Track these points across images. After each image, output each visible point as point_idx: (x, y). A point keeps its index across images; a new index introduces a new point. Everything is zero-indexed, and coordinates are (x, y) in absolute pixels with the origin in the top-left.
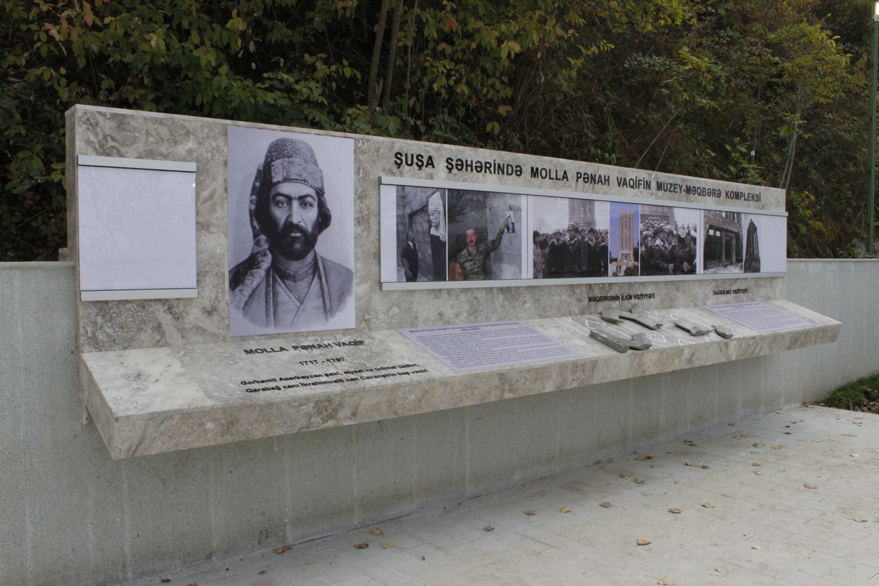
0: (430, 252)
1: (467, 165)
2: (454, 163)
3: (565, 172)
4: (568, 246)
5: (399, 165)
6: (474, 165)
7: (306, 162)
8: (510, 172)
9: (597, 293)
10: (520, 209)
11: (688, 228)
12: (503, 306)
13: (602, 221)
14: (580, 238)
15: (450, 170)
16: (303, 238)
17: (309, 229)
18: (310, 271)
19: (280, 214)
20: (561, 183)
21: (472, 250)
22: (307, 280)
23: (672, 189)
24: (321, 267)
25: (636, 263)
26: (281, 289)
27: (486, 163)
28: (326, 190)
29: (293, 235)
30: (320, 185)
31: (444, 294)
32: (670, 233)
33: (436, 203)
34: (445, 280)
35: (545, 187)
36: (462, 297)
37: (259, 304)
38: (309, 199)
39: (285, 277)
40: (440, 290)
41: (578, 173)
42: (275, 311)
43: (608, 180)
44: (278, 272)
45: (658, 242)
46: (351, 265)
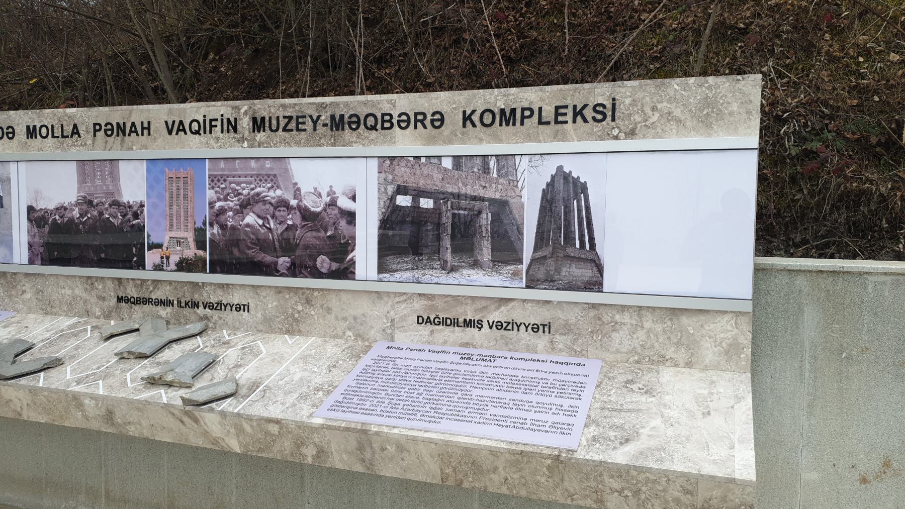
3: (75, 126)
4: (77, 225)
9: (132, 292)
10: (9, 180)
11: (331, 193)
13: (133, 186)
14: (95, 213)
20: (69, 141)
23: (292, 125)
25: (200, 253)
32: (283, 204)
41: (95, 125)
43: (149, 128)
45: (250, 219)
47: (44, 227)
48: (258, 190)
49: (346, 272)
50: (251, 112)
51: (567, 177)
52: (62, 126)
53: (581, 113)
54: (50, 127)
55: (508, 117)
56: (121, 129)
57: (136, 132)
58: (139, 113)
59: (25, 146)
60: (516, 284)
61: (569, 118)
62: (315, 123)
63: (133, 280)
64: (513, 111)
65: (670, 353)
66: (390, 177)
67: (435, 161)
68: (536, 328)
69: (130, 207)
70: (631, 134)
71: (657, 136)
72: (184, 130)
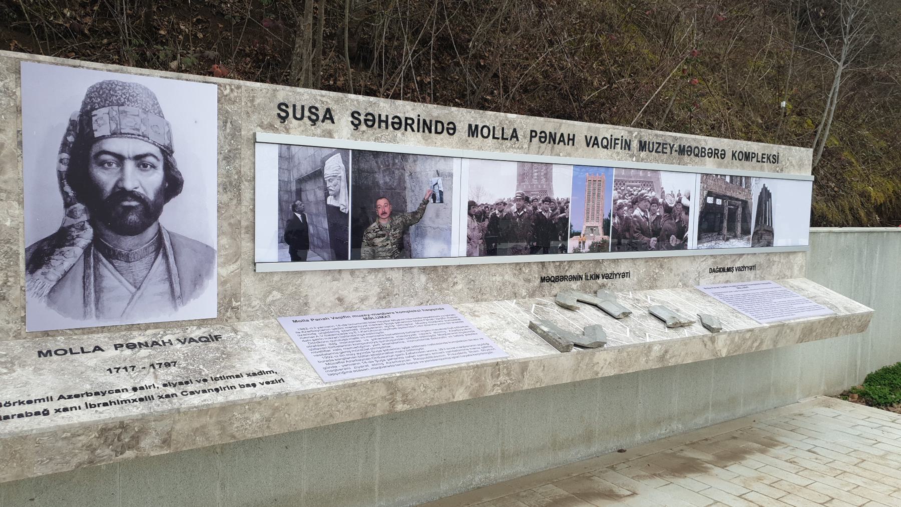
0: (326, 225)
1: (380, 121)
2: (362, 118)
3: (515, 130)
4: (514, 218)
5: (283, 119)
6: (390, 121)
7: (145, 111)
8: (439, 129)
9: (552, 272)
10: (451, 175)
11: (679, 195)
12: (426, 289)
13: (562, 188)
15: (356, 126)
16: (140, 209)
17: (151, 196)
18: (152, 249)
19: (106, 178)
20: (508, 143)
21: (385, 223)
22: (148, 259)
23: (660, 149)
24: (167, 244)
26: (107, 270)
27: (406, 119)
28: (176, 148)
29: (126, 203)
30: (167, 143)
31: (346, 277)
32: (655, 201)
33: (334, 167)
34: (346, 259)
35: (487, 148)
36: (371, 278)
37: (73, 292)
38: (150, 159)
39: (112, 255)
40: (340, 271)
41: (532, 131)
42: (97, 300)
43: (573, 140)
44: (101, 249)
45: (637, 212)
46: (212, 240)
47: (484, 220)
48: (643, 191)
52: (503, 129)
57: (564, 141)
58: (567, 127)
59: (464, 144)
63: (553, 262)
69: (559, 203)
72: (597, 144)
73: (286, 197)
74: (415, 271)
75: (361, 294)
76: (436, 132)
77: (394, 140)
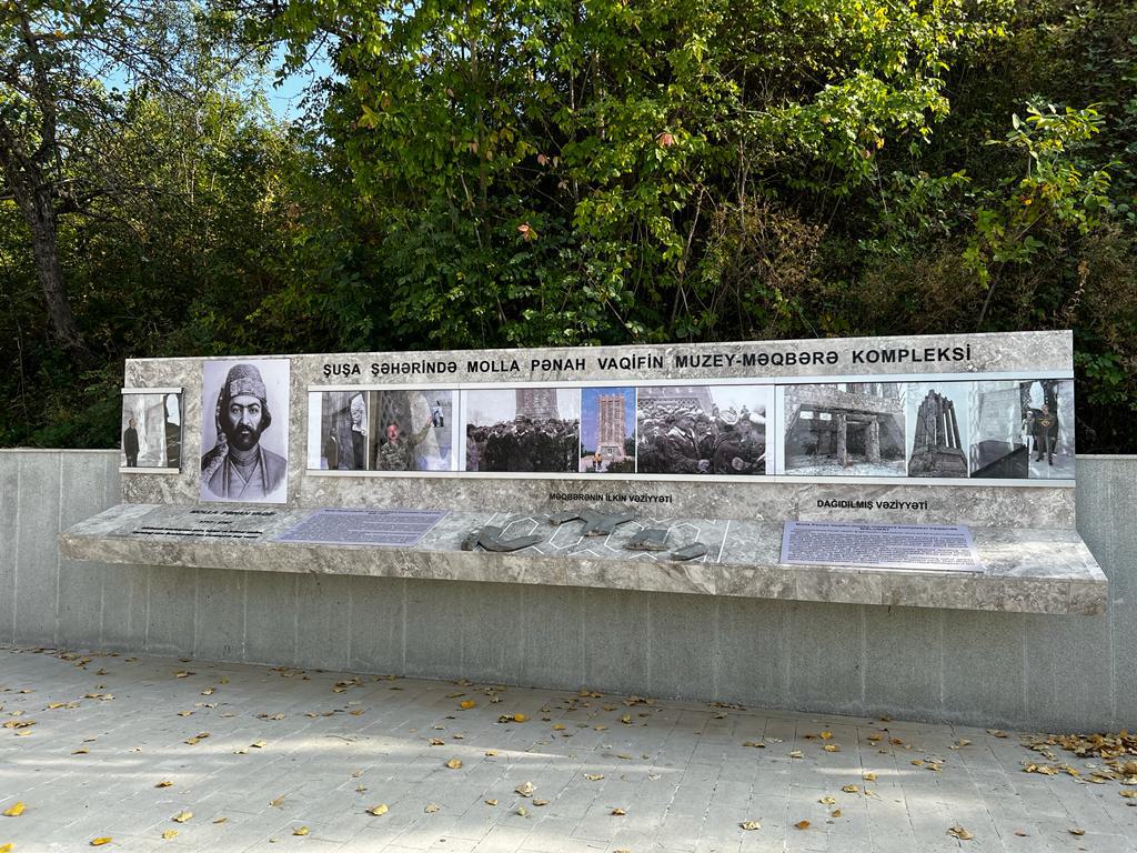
1: (393, 368)
2: (379, 368)
3: (515, 362)
4: (515, 439)
5: (328, 375)
8: (442, 369)
10: (450, 404)
13: (569, 409)
19: (235, 418)
20: (509, 374)
23: (711, 361)
26: (234, 470)
32: (701, 418)
35: (486, 381)
38: (255, 407)
39: (236, 462)
40: (364, 478)
43: (583, 364)
44: (232, 459)
45: (674, 431)
49: (759, 468)
50: (675, 352)
51: (937, 397)
53: (944, 353)
54: (490, 363)
55: (888, 356)
56: (558, 365)
57: (571, 366)
58: (574, 353)
60: (900, 473)
61: (936, 357)
62: (730, 360)
63: (565, 480)
64: (893, 352)
65: (1017, 518)
66: (795, 398)
67: (833, 386)
68: (915, 506)
69: (566, 424)
70: (982, 368)
71: (1000, 371)
72: (615, 365)
73: (326, 426)
74: (422, 481)
75: (380, 497)
76: (439, 371)
77: (404, 382)
